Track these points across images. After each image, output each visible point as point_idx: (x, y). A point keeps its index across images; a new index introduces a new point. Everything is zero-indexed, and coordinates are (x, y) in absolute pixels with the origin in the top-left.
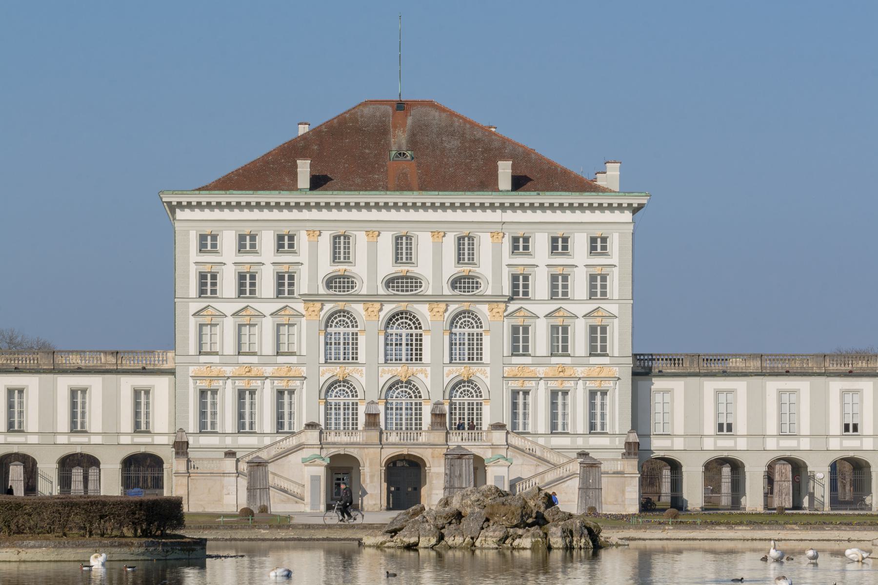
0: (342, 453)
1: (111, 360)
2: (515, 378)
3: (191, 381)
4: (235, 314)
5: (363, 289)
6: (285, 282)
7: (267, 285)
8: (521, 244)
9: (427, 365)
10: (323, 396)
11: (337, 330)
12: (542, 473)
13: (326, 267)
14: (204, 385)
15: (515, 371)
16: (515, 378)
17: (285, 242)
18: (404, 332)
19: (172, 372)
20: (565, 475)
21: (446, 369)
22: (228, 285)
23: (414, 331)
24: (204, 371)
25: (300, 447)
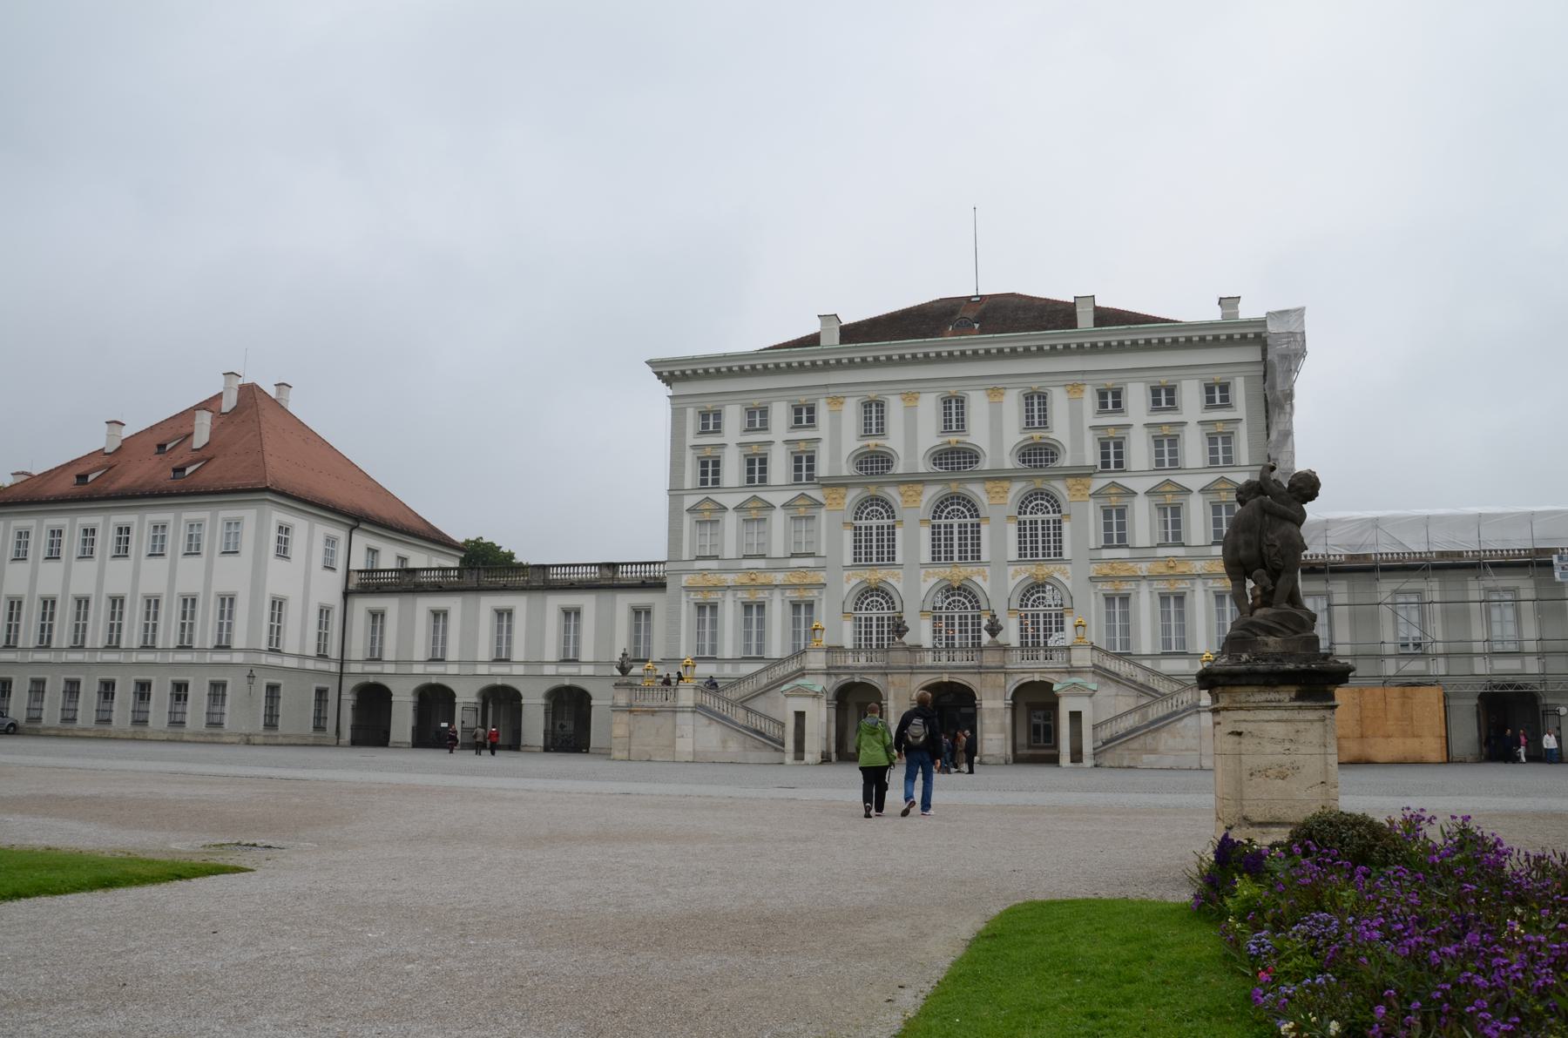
0: (857, 680)
1: (608, 573)
2: (1106, 578)
3: (684, 594)
4: (738, 509)
5: (899, 468)
6: (803, 463)
7: (780, 468)
8: (1111, 400)
9: (988, 564)
10: (849, 608)
11: (869, 523)
12: (1144, 706)
13: (851, 442)
14: (699, 597)
15: (1106, 570)
16: (1106, 578)
17: (804, 415)
18: (956, 521)
19: (658, 585)
20: (1181, 708)
21: (1011, 570)
22: (733, 471)
23: (969, 520)
24: (698, 580)
25: (802, 673)
